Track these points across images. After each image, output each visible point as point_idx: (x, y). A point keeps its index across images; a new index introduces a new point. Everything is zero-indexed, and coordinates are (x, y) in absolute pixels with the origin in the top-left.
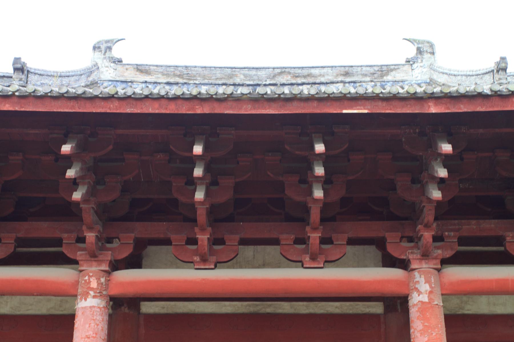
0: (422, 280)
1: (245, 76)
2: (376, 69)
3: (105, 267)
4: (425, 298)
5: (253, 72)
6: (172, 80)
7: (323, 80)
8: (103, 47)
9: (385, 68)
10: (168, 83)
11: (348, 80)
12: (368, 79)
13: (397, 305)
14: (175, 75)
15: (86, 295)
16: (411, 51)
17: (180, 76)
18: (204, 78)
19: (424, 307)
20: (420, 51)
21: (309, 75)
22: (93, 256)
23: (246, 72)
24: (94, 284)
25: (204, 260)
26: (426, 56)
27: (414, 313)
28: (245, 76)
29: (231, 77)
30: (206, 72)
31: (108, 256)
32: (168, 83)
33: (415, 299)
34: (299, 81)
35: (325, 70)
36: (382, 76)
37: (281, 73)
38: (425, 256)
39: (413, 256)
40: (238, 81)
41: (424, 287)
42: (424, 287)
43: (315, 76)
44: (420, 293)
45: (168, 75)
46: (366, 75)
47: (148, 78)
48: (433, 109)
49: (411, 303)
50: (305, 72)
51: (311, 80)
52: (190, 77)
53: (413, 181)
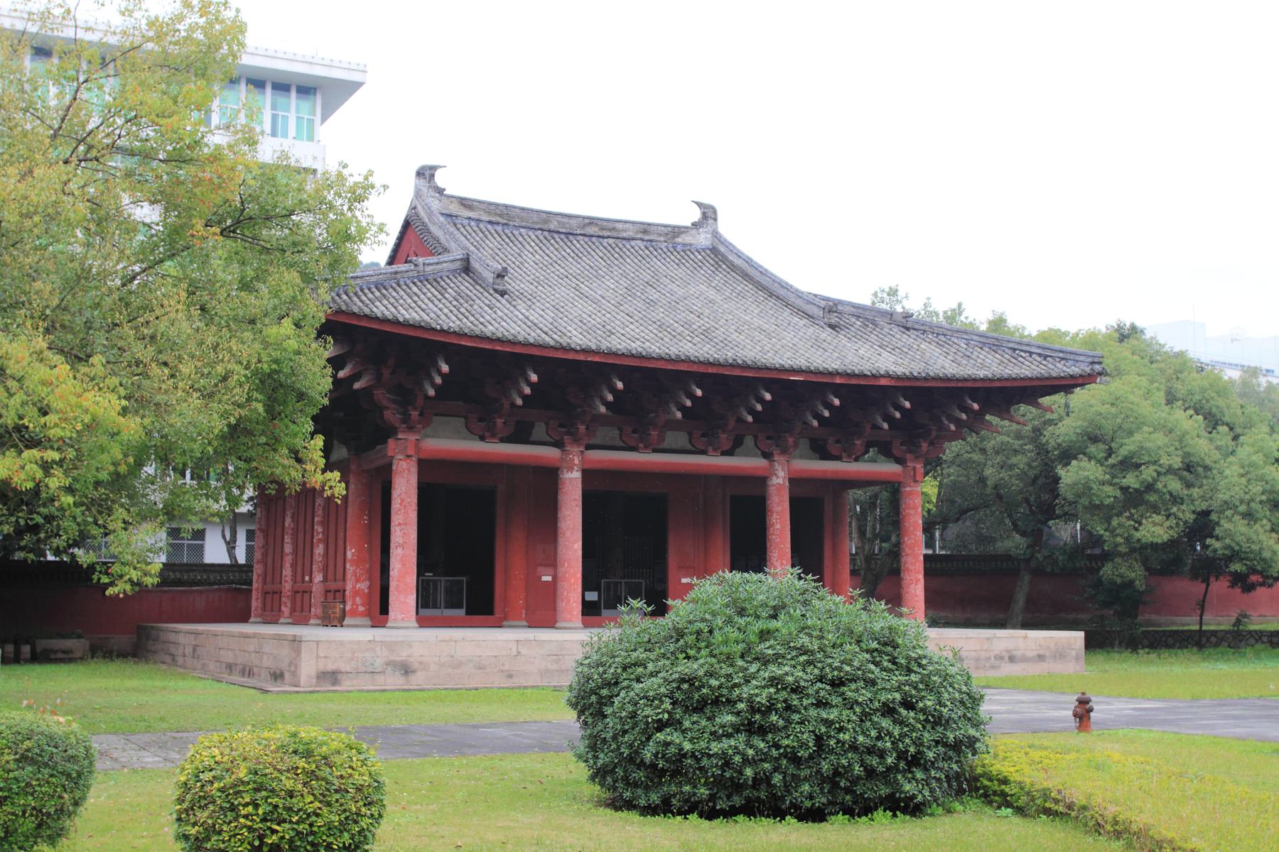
1: (559, 223)
4: (780, 481)
5: (566, 220)
6: (493, 219)
7: (625, 235)
8: (427, 173)
10: (490, 222)
11: (646, 238)
13: (761, 481)
14: (496, 214)
15: (571, 469)
16: (696, 215)
17: (500, 215)
18: (522, 219)
19: (780, 487)
20: (704, 214)
21: (614, 229)
23: (559, 218)
24: (576, 462)
26: (711, 221)
28: (559, 223)
29: (546, 221)
30: (524, 215)
32: (490, 222)
34: (606, 233)
35: (627, 226)
40: (552, 227)
41: (781, 474)
42: (781, 474)
45: (489, 213)
47: (471, 214)
48: (838, 381)
49: (769, 483)
50: (610, 225)
51: (615, 234)
52: (511, 218)
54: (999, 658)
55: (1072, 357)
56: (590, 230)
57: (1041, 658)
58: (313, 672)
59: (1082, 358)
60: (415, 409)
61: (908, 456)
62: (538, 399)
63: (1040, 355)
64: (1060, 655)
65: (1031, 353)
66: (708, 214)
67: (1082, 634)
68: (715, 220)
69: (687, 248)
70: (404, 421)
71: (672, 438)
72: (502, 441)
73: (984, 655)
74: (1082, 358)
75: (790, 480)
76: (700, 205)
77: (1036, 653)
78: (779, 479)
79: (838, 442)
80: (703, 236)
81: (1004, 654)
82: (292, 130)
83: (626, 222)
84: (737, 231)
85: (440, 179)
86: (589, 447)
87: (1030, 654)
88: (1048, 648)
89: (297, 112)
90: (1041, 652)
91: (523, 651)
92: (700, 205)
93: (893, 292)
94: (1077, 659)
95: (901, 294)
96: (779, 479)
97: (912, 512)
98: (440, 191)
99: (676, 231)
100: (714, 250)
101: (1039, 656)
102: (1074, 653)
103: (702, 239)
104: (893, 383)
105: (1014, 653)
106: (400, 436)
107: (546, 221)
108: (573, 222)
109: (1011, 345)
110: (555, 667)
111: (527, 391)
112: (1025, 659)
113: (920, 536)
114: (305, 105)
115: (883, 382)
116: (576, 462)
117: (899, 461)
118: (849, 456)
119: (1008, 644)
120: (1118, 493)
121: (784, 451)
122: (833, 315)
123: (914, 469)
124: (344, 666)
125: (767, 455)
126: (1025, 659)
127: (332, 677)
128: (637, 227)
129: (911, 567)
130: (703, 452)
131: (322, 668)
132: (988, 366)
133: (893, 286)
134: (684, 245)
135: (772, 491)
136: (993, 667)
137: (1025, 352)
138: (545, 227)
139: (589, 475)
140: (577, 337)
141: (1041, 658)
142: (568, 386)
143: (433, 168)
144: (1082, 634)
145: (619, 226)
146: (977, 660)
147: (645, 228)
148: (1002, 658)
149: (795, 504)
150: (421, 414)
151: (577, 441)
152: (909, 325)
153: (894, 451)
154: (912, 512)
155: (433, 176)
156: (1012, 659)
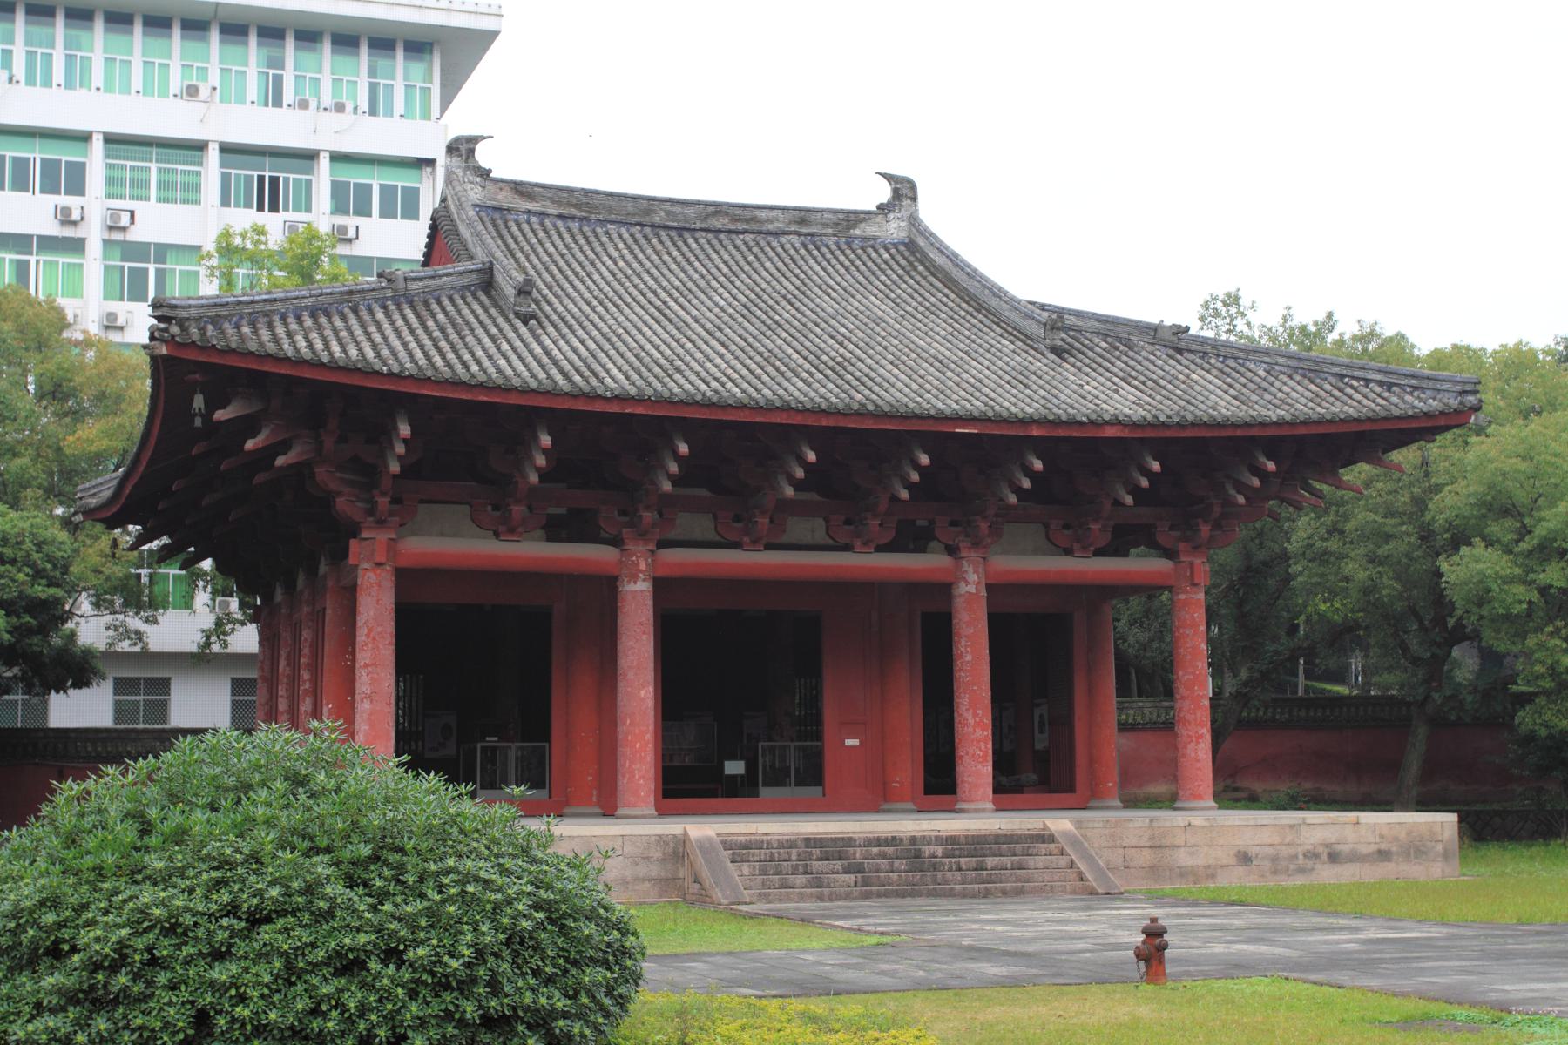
0: (971, 569)
1: (667, 213)
2: (841, 216)
3: (652, 547)
5: (678, 209)
6: (565, 212)
7: (770, 227)
8: (463, 148)
9: (852, 217)
10: (561, 217)
11: (804, 230)
12: (830, 231)
13: (944, 590)
14: (570, 205)
15: (634, 578)
16: (884, 193)
17: (576, 206)
18: (610, 210)
20: (897, 195)
21: (754, 219)
24: (643, 566)
26: (906, 202)
28: (667, 213)
29: (648, 212)
30: (613, 203)
32: (561, 217)
34: (741, 226)
36: (848, 228)
37: (715, 213)
39: (964, 544)
40: (657, 220)
41: (973, 577)
42: (973, 577)
43: (760, 221)
44: (967, 583)
45: (559, 203)
46: (826, 225)
47: (531, 206)
48: (1035, 432)
50: (748, 214)
51: (755, 227)
52: (592, 209)
54: (1312, 855)
55: (1430, 384)
56: (717, 223)
57: (1383, 855)
59: (1446, 386)
60: (383, 494)
61: (1182, 546)
62: (816, 478)
63: (1381, 383)
64: (1416, 849)
65: (1367, 381)
66: (903, 191)
67: (1454, 817)
68: (914, 199)
69: (870, 243)
70: (371, 512)
71: (799, 528)
72: (879, 549)
74: (1446, 386)
75: (989, 587)
76: (889, 178)
77: (1373, 848)
78: (971, 585)
79: (1066, 527)
80: (894, 225)
81: (1320, 849)
82: (399, 105)
83: (772, 208)
84: (947, 219)
85: (484, 156)
86: (663, 544)
87: (1365, 850)
88: (1396, 839)
89: (406, 78)
90: (1383, 847)
92: (889, 178)
93: (1233, 300)
94: (1446, 856)
95: (1245, 302)
96: (971, 585)
97: (1189, 631)
98: (485, 174)
99: (850, 219)
100: (911, 245)
101: (1380, 852)
102: (1440, 847)
103: (894, 229)
104: (1126, 434)
105: (1339, 848)
106: (364, 535)
107: (648, 212)
108: (690, 211)
109: (1336, 370)
111: (915, 477)
112: (1355, 857)
114: (417, 68)
115: (1110, 432)
116: (643, 566)
117: (1170, 554)
118: (1084, 548)
119: (1330, 835)
120: (1535, 596)
121: (976, 544)
122: (1063, 334)
123: (1191, 565)
125: (952, 551)
126: (1355, 857)
128: (788, 216)
129: (1189, 717)
130: (847, 548)
132: (1296, 401)
133: (1233, 290)
134: (865, 239)
135: (959, 603)
136: (1301, 871)
137: (1358, 379)
138: (647, 220)
139: (663, 587)
140: (615, 378)
141: (1383, 855)
142: (609, 453)
143: (474, 140)
144: (1454, 817)
145: (762, 214)
146: (1275, 859)
147: (802, 216)
149: (1001, 628)
150: (396, 500)
151: (642, 535)
152: (1182, 345)
153: (1161, 540)
154: (1189, 631)
155: (472, 152)
156: (1334, 857)
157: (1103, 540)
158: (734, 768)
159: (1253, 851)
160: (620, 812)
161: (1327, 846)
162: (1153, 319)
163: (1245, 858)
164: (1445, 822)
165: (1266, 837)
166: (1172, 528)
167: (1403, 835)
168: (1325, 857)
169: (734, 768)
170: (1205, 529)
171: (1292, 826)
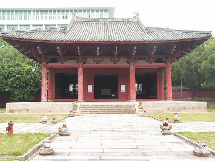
13: (129, 69)
22: (81, 62)
25: (98, 62)
27: (130, 70)
31: (83, 62)
33: (131, 68)
38: (133, 62)
53: (131, 50)
58: (9, 110)
61: (166, 61)
64: (199, 108)
66: (137, 14)
73: (176, 108)
77: (192, 107)
78: (132, 68)
90: (193, 107)
91: (53, 106)
101: (193, 108)
102: (204, 107)
110: (61, 110)
112: (188, 109)
113: (163, 78)
117: (165, 62)
119: (184, 105)
122: (149, 31)
123: (168, 64)
124: (14, 109)
126: (188, 109)
127: (12, 111)
131: (10, 109)
136: (178, 111)
146: (174, 109)
148: (182, 108)
156: (184, 109)
157: (154, 60)
158: (113, 95)
159: (170, 108)
160: (78, 101)
161: (183, 107)
162: (164, 28)
163: (169, 109)
164: (205, 103)
165: (172, 105)
166: (166, 58)
167: (197, 105)
168: (183, 109)
169: (113, 95)
170: (170, 58)
171: (177, 104)
